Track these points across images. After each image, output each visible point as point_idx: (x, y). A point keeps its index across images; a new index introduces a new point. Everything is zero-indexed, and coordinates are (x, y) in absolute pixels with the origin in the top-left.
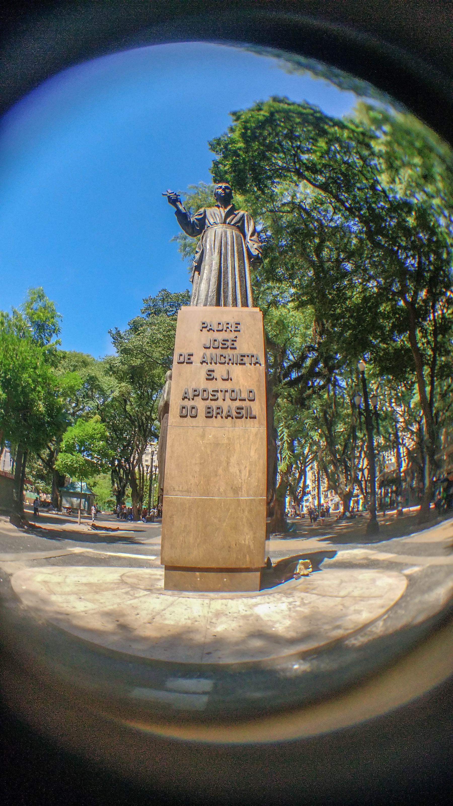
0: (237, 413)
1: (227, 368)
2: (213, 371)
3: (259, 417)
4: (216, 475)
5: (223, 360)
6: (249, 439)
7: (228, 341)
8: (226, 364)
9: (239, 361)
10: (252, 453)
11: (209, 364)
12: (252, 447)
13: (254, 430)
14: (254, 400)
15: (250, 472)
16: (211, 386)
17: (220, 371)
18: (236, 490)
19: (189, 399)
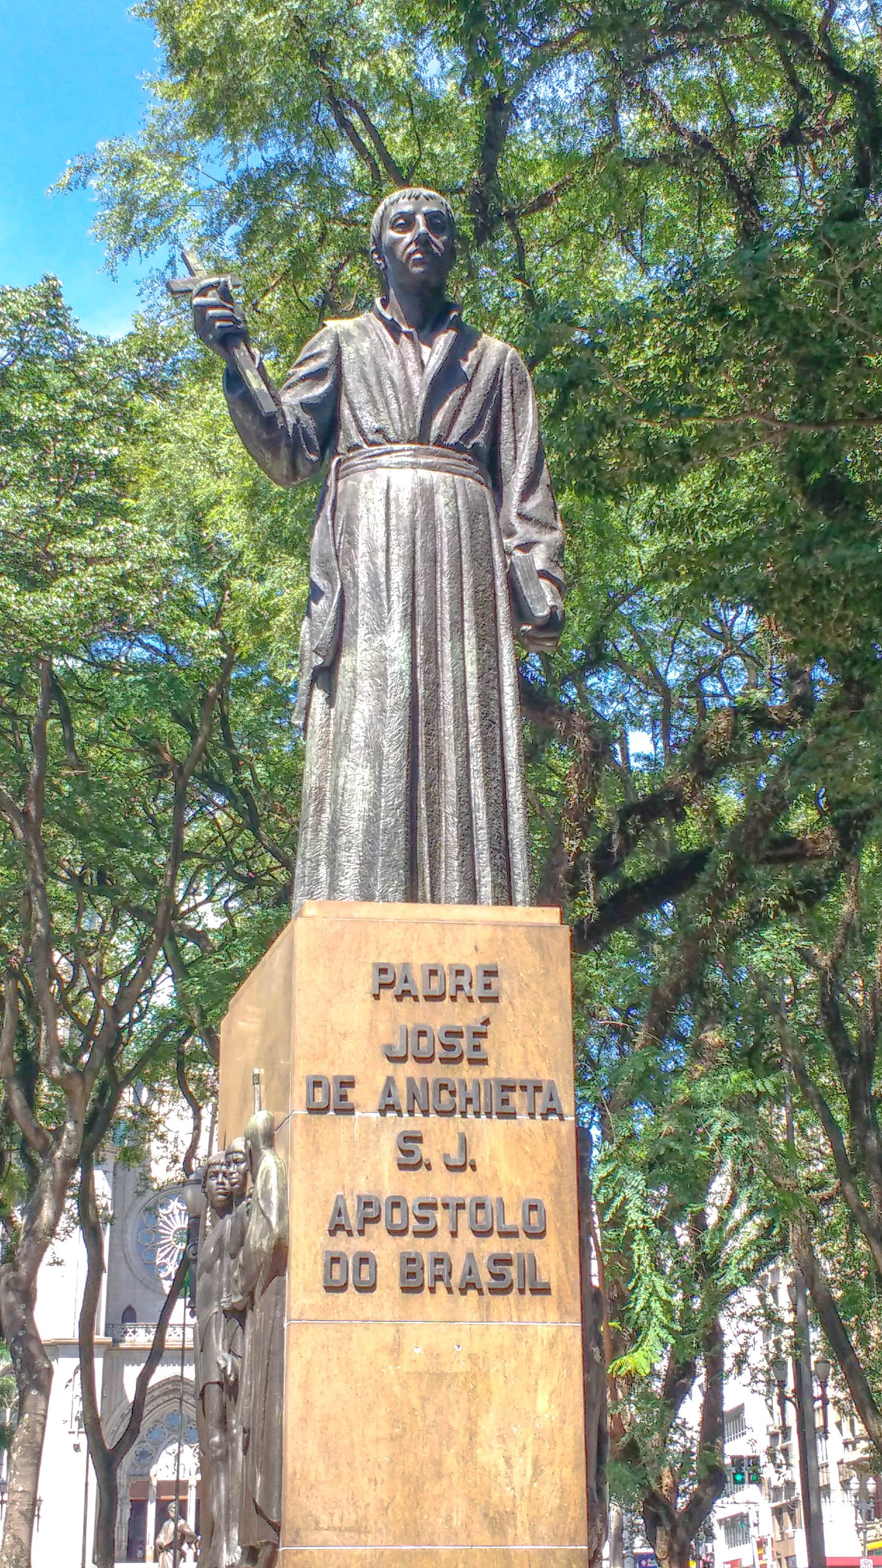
0: (494, 1276)
1: (462, 1129)
2: (419, 1139)
3: (559, 1290)
4: (439, 1475)
6: (529, 1359)
7: (460, 1034)
8: (458, 1116)
10: (542, 1403)
11: (406, 1115)
12: (540, 1382)
13: (545, 1331)
14: (541, 1235)
16: (414, 1188)
17: (440, 1136)
18: (498, 1522)
19: (350, 1233)
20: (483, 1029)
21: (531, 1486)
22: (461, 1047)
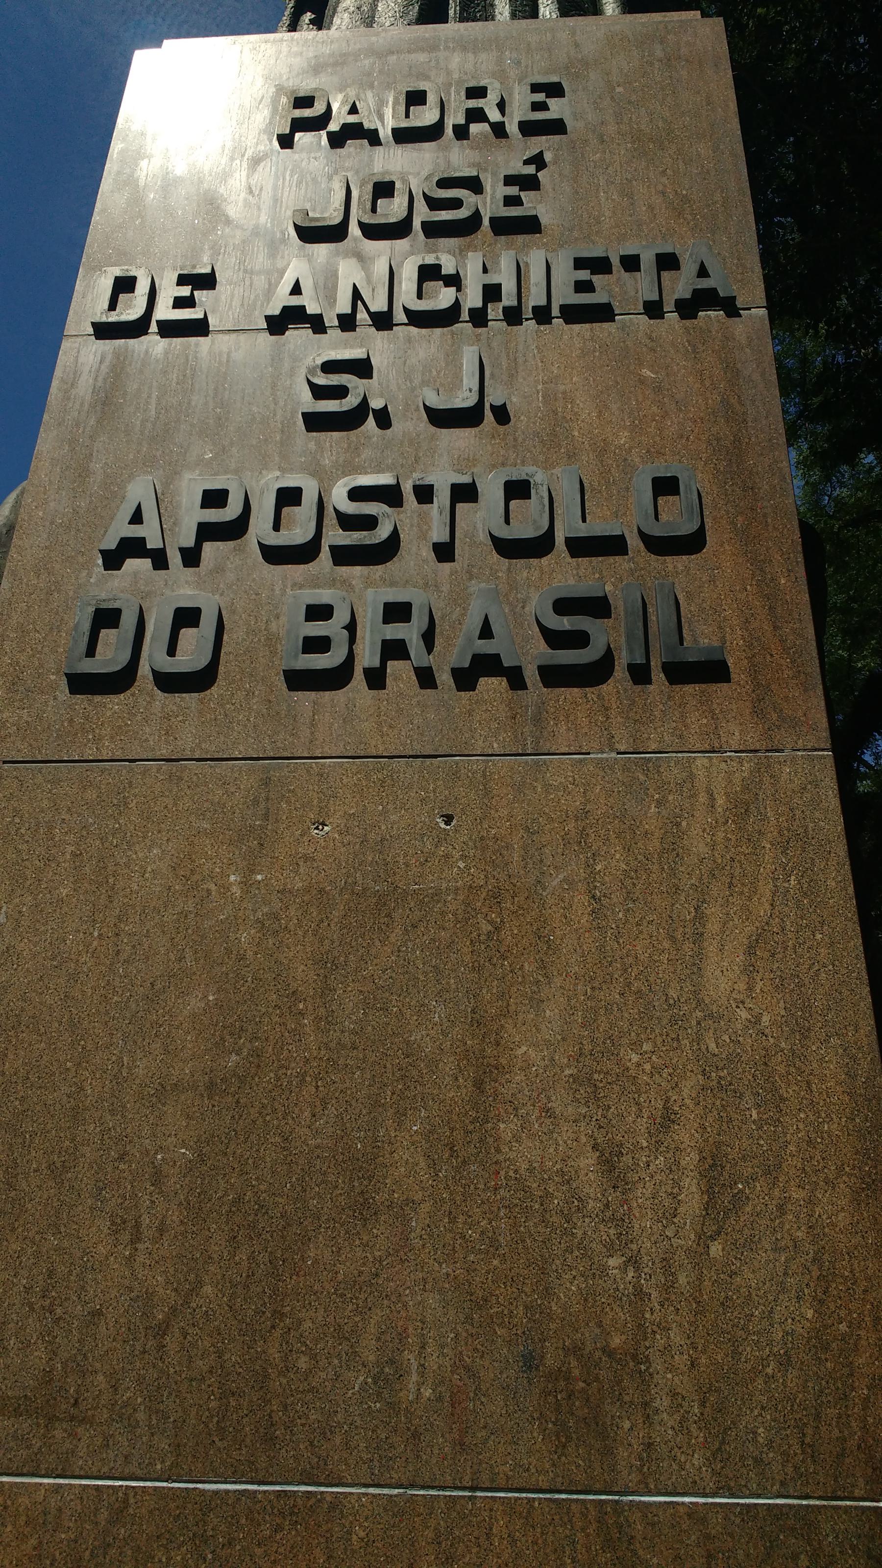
4: (364, 1209)
8: (464, 327)
9: (564, 294)
10: (722, 977)
12: (713, 910)
13: (718, 775)
14: (692, 544)
15: (713, 1167)
18: (580, 1393)
19: (160, 560)
20: (531, 170)
21: (699, 1255)
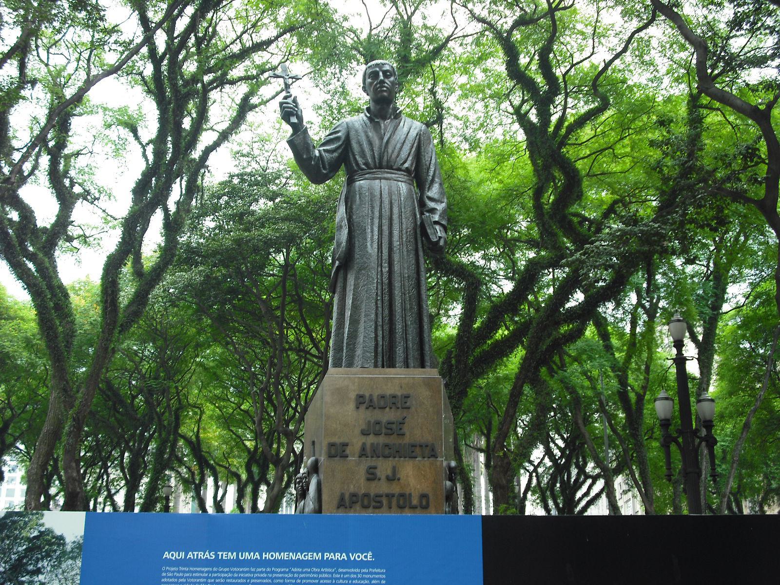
2: (375, 468)
5: (387, 452)
17: (384, 467)
22: (394, 429)
